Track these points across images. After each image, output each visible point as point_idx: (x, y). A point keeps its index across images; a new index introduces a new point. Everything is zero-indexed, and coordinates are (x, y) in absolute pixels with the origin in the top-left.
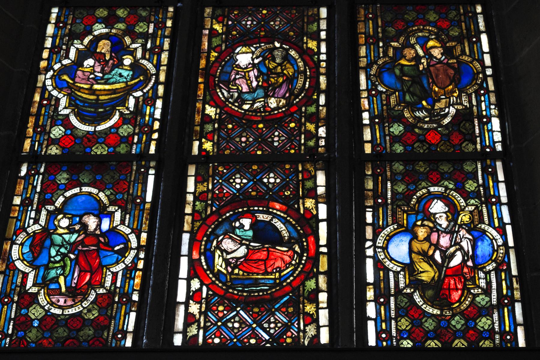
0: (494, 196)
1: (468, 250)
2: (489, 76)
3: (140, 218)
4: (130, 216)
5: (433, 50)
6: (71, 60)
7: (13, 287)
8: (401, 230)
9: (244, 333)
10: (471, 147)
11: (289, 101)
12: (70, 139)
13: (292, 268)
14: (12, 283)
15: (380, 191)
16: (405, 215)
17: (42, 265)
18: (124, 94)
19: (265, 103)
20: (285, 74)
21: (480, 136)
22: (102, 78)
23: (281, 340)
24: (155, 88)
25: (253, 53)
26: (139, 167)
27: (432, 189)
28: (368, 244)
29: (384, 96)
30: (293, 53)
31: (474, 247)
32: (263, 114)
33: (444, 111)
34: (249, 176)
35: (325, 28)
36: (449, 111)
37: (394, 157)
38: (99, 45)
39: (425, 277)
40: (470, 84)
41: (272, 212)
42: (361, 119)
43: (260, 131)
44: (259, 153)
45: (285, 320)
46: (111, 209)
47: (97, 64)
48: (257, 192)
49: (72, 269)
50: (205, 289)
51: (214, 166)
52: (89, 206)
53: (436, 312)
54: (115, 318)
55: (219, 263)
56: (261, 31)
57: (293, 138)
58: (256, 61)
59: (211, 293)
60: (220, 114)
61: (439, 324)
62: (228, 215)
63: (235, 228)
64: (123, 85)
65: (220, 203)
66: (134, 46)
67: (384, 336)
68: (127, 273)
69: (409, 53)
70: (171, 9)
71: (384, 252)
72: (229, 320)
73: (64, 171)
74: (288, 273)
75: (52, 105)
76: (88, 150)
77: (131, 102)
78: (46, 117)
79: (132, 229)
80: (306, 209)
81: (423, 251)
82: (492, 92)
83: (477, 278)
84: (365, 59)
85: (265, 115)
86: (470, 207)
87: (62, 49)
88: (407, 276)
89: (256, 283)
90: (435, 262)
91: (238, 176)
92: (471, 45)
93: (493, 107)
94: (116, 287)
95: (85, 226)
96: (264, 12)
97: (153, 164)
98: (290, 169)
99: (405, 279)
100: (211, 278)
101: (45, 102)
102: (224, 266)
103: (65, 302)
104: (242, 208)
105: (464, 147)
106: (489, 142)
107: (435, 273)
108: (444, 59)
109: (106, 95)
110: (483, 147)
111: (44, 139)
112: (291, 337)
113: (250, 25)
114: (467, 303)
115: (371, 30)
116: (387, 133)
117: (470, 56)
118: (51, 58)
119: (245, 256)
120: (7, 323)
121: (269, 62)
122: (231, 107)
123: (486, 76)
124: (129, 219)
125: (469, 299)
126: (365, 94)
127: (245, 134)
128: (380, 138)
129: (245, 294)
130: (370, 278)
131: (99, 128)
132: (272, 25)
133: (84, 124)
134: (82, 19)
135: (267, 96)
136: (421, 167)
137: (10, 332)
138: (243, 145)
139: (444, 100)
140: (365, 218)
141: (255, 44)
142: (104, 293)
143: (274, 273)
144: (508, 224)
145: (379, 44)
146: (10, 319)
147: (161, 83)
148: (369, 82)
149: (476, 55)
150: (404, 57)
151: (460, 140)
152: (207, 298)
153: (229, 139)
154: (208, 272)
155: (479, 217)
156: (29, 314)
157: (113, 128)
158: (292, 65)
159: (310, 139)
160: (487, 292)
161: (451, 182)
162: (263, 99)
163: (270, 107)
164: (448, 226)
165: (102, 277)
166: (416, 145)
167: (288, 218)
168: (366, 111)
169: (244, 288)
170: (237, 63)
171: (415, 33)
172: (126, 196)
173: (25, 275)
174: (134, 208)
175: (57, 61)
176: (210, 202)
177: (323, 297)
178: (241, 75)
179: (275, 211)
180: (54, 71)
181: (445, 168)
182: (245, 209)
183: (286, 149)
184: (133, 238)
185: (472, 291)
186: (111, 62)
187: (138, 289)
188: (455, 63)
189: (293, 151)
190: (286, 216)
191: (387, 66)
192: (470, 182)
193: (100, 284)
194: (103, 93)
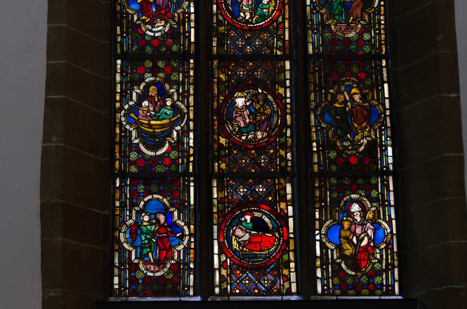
0: (387, 201)
1: (371, 236)
2: (388, 116)
3: (189, 215)
4: (183, 214)
5: (355, 95)
6: (134, 102)
7: (125, 259)
8: (335, 223)
9: (252, 287)
10: (375, 166)
11: (269, 134)
12: (142, 161)
13: (275, 247)
14: (124, 257)
15: (323, 197)
16: (337, 213)
17: (139, 246)
18: (170, 128)
19: (255, 135)
20: (265, 113)
21: (381, 160)
22: (155, 116)
23: (271, 291)
24: (187, 124)
25: (245, 97)
26: (184, 181)
27: (352, 196)
28: (317, 232)
29: (325, 130)
30: (270, 97)
31: (374, 234)
32: (254, 143)
33: (360, 142)
34: (248, 187)
35: (289, 78)
36: (363, 142)
37: (331, 174)
38: (150, 90)
39: (347, 253)
40: (376, 122)
41: (262, 211)
42: (312, 147)
43: (253, 155)
44: (253, 171)
45: (272, 279)
46: (172, 209)
47: (150, 105)
48: (253, 198)
49: (155, 248)
50: (228, 260)
51: (227, 180)
52: (159, 207)
53: (353, 273)
54: (182, 278)
55: (235, 243)
56: (250, 80)
57: (272, 161)
58: (248, 104)
59: (232, 262)
60: (229, 143)
61: (355, 281)
62: (237, 213)
63: (242, 221)
64: (167, 121)
65: (233, 206)
66: (172, 91)
67: (325, 288)
68: (185, 251)
69: (340, 98)
70: (192, 61)
71: (325, 237)
72: (243, 279)
73: (141, 184)
74: (273, 250)
75: (128, 136)
76: (153, 169)
77: (175, 134)
78: (125, 145)
79: (185, 222)
80: (281, 209)
81: (347, 236)
82: (389, 127)
83: (375, 253)
84: (314, 103)
85: (255, 144)
86: (373, 208)
87: (127, 93)
88: (338, 252)
89: (256, 256)
90: (353, 243)
91: (241, 187)
92: (378, 92)
93: (389, 139)
94: (180, 260)
95: (158, 221)
96: (251, 64)
97: (192, 179)
98: (271, 182)
99: (337, 253)
100: (231, 254)
101: (123, 134)
102: (238, 246)
103: (154, 268)
104: (245, 209)
105: (371, 167)
106: (386, 164)
107: (353, 250)
108: (361, 103)
109: (159, 128)
110: (382, 168)
111: (127, 161)
112: (276, 289)
113: (242, 75)
114: (370, 268)
115: (317, 80)
116: (327, 157)
117: (377, 101)
118: (122, 101)
119: (249, 240)
120: (125, 281)
121: (255, 104)
122: (234, 138)
123: (386, 116)
124: (183, 216)
125: (371, 266)
126: (314, 130)
127: (244, 158)
128: (323, 160)
129: (250, 263)
130: (318, 253)
131: (159, 153)
132: (256, 75)
133: (149, 151)
134: (137, 69)
135: (255, 130)
136: (346, 181)
137: (128, 286)
138: (244, 165)
139: (360, 134)
140: (315, 216)
141: (247, 90)
142: (174, 264)
143: (265, 250)
144: (394, 219)
145: (322, 91)
146: (126, 279)
147: (191, 120)
148: (316, 120)
149: (381, 100)
150: (337, 101)
151: (369, 162)
152: (230, 266)
153: (235, 162)
154: (229, 250)
155: (378, 214)
156: (136, 276)
157: (166, 153)
158: (269, 106)
159: (283, 162)
160: (380, 261)
161: (363, 191)
162: (253, 133)
163: (258, 138)
164: (361, 220)
165: (172, 254)
166: (343, 166)
167: (271, 215)
168: (315, 141)
169: (249, 259)
170: (236, 105)
171: (344, 83)
172: (179, 201)
173: (130, 252)
174: (184, 209)
175: (126, 103)
176: (227, 205)
177: (292, 265)
178: (239, 114)
179: (263, 210)
180: (125, 110)
181: (360, 181)
182: (247, 209)
183: (269, 168)
184: (186, 228)
185: (372, 261)
186: (159, 103)
187: (193, 260)
188: (367, 106)
189: (272, 170)
190: (270, 213)
191: (327, 108)
192: (374, 191)
193: (172, 258)
194: (157, 127)
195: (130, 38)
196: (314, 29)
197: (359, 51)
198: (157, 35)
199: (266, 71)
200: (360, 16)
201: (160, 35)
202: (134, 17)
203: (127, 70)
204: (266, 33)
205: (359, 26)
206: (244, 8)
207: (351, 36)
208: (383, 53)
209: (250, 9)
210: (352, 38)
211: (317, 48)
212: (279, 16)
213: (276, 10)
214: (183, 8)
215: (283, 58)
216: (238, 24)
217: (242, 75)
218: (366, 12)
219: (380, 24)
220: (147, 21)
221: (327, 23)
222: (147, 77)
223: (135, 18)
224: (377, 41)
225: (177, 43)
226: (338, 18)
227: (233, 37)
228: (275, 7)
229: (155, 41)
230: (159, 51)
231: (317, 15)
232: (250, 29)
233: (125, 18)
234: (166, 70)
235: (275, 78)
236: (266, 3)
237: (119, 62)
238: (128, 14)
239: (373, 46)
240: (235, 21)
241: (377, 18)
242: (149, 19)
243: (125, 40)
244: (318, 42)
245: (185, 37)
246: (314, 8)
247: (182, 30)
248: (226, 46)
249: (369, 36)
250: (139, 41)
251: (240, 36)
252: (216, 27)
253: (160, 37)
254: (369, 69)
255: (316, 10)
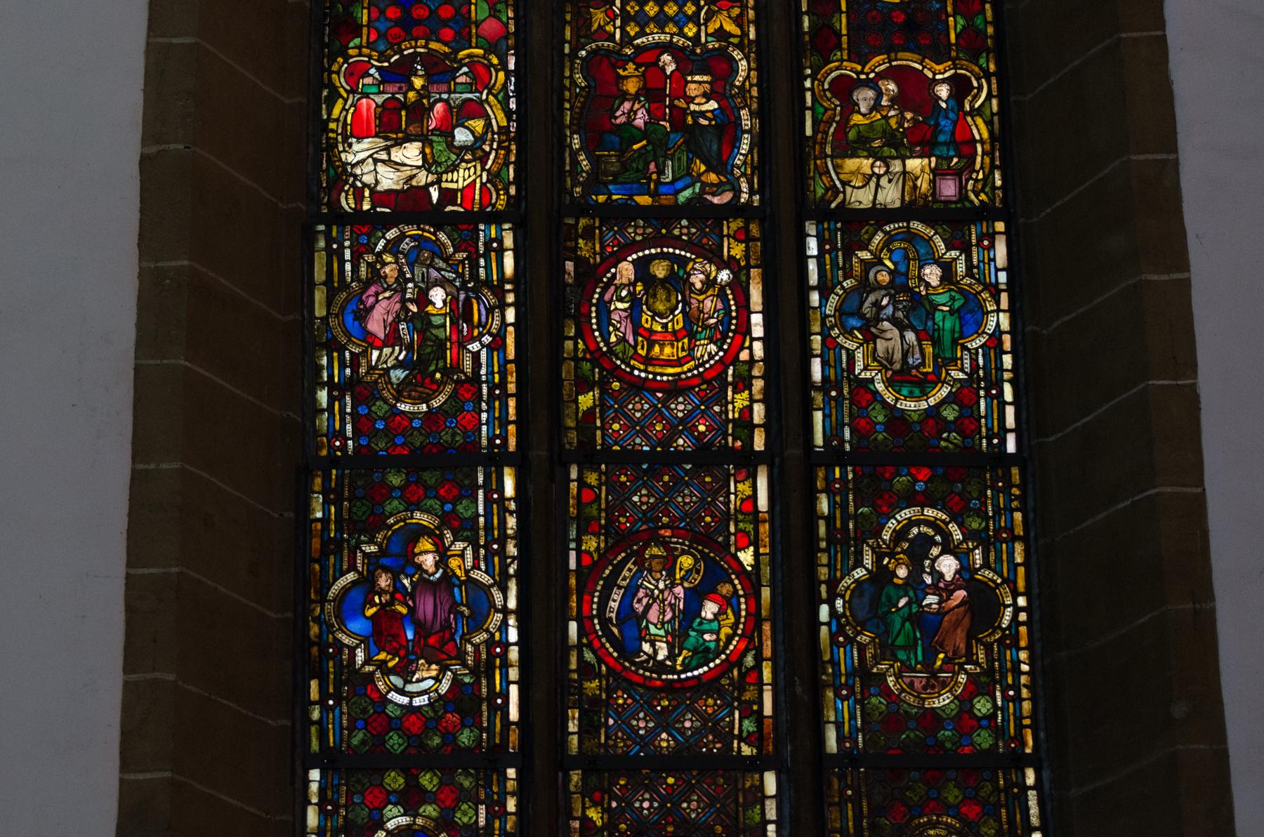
35: (774, 818)
56: (668, 823)
70: (511, 773)
96: (671, 780)
113: (648, 809)
115: (851, 824)
132: (684, 809)
195: (345, 710)
196: (842, 687)
197: (961, 745)
198: (417, 702)
199: (713, 800)
200: (964, 651)
201: (427, 702)
202: (355, 655)
203: (336, 796)
204: (712, 698)
205: (962, 678)
206: (653, 630)
207: (942, 704)
208: (1028, 751)
209: (667, 632)
210: (944, 711)
211: (850, 738)
212: (746, 651)
213: (738, 635)
214: (487, 631)
215: (757, 765)
216: (636, 672)
217: (647, 809)
218: (979, 641)
219: (1017, 672)
220: (391, 664)
221: (875, 670)
222: (389, 815)
223: (360, 656)
224: (1012, 718)
225: (473, 725)
226: (905, 658)
227: (624, 709)
228: (735, 626)
229: (413, 718)
230: (422, 746)
231: (848, 648)
232: (670, 688)
233: (332, 657)
234: (442, 796)
235: (737, 818)
236: (710, 616)
237: (315, 775)
238: (339, 646)
239: (1000, 732)
240: (627, 664)
241: (1008, 658)
242: (397, 659)
243: (331, 716)
244: (853, 722)
245: (493, 708)
246: (841, 630)
247: (484, 690)
248: (603, 731)
249: (989, 706)
250: (370, 720)
251: (641, 705)
252: (575, 681)
253: (426, 709)
254: (992, 793)
255: (846, 636)
